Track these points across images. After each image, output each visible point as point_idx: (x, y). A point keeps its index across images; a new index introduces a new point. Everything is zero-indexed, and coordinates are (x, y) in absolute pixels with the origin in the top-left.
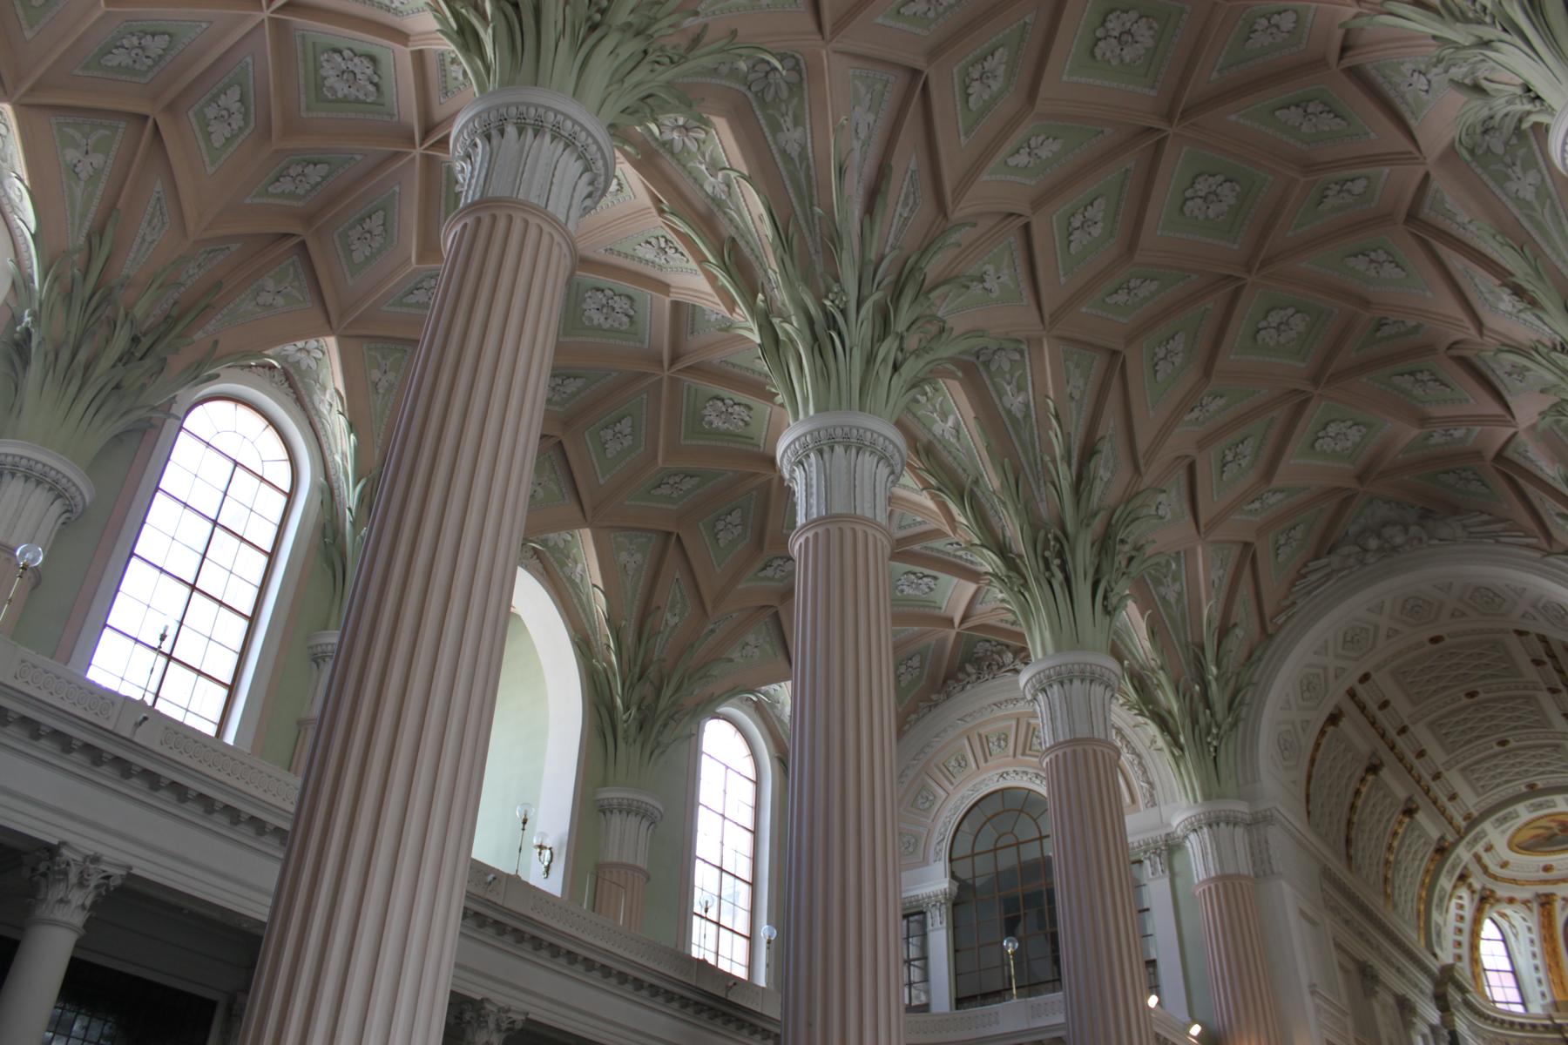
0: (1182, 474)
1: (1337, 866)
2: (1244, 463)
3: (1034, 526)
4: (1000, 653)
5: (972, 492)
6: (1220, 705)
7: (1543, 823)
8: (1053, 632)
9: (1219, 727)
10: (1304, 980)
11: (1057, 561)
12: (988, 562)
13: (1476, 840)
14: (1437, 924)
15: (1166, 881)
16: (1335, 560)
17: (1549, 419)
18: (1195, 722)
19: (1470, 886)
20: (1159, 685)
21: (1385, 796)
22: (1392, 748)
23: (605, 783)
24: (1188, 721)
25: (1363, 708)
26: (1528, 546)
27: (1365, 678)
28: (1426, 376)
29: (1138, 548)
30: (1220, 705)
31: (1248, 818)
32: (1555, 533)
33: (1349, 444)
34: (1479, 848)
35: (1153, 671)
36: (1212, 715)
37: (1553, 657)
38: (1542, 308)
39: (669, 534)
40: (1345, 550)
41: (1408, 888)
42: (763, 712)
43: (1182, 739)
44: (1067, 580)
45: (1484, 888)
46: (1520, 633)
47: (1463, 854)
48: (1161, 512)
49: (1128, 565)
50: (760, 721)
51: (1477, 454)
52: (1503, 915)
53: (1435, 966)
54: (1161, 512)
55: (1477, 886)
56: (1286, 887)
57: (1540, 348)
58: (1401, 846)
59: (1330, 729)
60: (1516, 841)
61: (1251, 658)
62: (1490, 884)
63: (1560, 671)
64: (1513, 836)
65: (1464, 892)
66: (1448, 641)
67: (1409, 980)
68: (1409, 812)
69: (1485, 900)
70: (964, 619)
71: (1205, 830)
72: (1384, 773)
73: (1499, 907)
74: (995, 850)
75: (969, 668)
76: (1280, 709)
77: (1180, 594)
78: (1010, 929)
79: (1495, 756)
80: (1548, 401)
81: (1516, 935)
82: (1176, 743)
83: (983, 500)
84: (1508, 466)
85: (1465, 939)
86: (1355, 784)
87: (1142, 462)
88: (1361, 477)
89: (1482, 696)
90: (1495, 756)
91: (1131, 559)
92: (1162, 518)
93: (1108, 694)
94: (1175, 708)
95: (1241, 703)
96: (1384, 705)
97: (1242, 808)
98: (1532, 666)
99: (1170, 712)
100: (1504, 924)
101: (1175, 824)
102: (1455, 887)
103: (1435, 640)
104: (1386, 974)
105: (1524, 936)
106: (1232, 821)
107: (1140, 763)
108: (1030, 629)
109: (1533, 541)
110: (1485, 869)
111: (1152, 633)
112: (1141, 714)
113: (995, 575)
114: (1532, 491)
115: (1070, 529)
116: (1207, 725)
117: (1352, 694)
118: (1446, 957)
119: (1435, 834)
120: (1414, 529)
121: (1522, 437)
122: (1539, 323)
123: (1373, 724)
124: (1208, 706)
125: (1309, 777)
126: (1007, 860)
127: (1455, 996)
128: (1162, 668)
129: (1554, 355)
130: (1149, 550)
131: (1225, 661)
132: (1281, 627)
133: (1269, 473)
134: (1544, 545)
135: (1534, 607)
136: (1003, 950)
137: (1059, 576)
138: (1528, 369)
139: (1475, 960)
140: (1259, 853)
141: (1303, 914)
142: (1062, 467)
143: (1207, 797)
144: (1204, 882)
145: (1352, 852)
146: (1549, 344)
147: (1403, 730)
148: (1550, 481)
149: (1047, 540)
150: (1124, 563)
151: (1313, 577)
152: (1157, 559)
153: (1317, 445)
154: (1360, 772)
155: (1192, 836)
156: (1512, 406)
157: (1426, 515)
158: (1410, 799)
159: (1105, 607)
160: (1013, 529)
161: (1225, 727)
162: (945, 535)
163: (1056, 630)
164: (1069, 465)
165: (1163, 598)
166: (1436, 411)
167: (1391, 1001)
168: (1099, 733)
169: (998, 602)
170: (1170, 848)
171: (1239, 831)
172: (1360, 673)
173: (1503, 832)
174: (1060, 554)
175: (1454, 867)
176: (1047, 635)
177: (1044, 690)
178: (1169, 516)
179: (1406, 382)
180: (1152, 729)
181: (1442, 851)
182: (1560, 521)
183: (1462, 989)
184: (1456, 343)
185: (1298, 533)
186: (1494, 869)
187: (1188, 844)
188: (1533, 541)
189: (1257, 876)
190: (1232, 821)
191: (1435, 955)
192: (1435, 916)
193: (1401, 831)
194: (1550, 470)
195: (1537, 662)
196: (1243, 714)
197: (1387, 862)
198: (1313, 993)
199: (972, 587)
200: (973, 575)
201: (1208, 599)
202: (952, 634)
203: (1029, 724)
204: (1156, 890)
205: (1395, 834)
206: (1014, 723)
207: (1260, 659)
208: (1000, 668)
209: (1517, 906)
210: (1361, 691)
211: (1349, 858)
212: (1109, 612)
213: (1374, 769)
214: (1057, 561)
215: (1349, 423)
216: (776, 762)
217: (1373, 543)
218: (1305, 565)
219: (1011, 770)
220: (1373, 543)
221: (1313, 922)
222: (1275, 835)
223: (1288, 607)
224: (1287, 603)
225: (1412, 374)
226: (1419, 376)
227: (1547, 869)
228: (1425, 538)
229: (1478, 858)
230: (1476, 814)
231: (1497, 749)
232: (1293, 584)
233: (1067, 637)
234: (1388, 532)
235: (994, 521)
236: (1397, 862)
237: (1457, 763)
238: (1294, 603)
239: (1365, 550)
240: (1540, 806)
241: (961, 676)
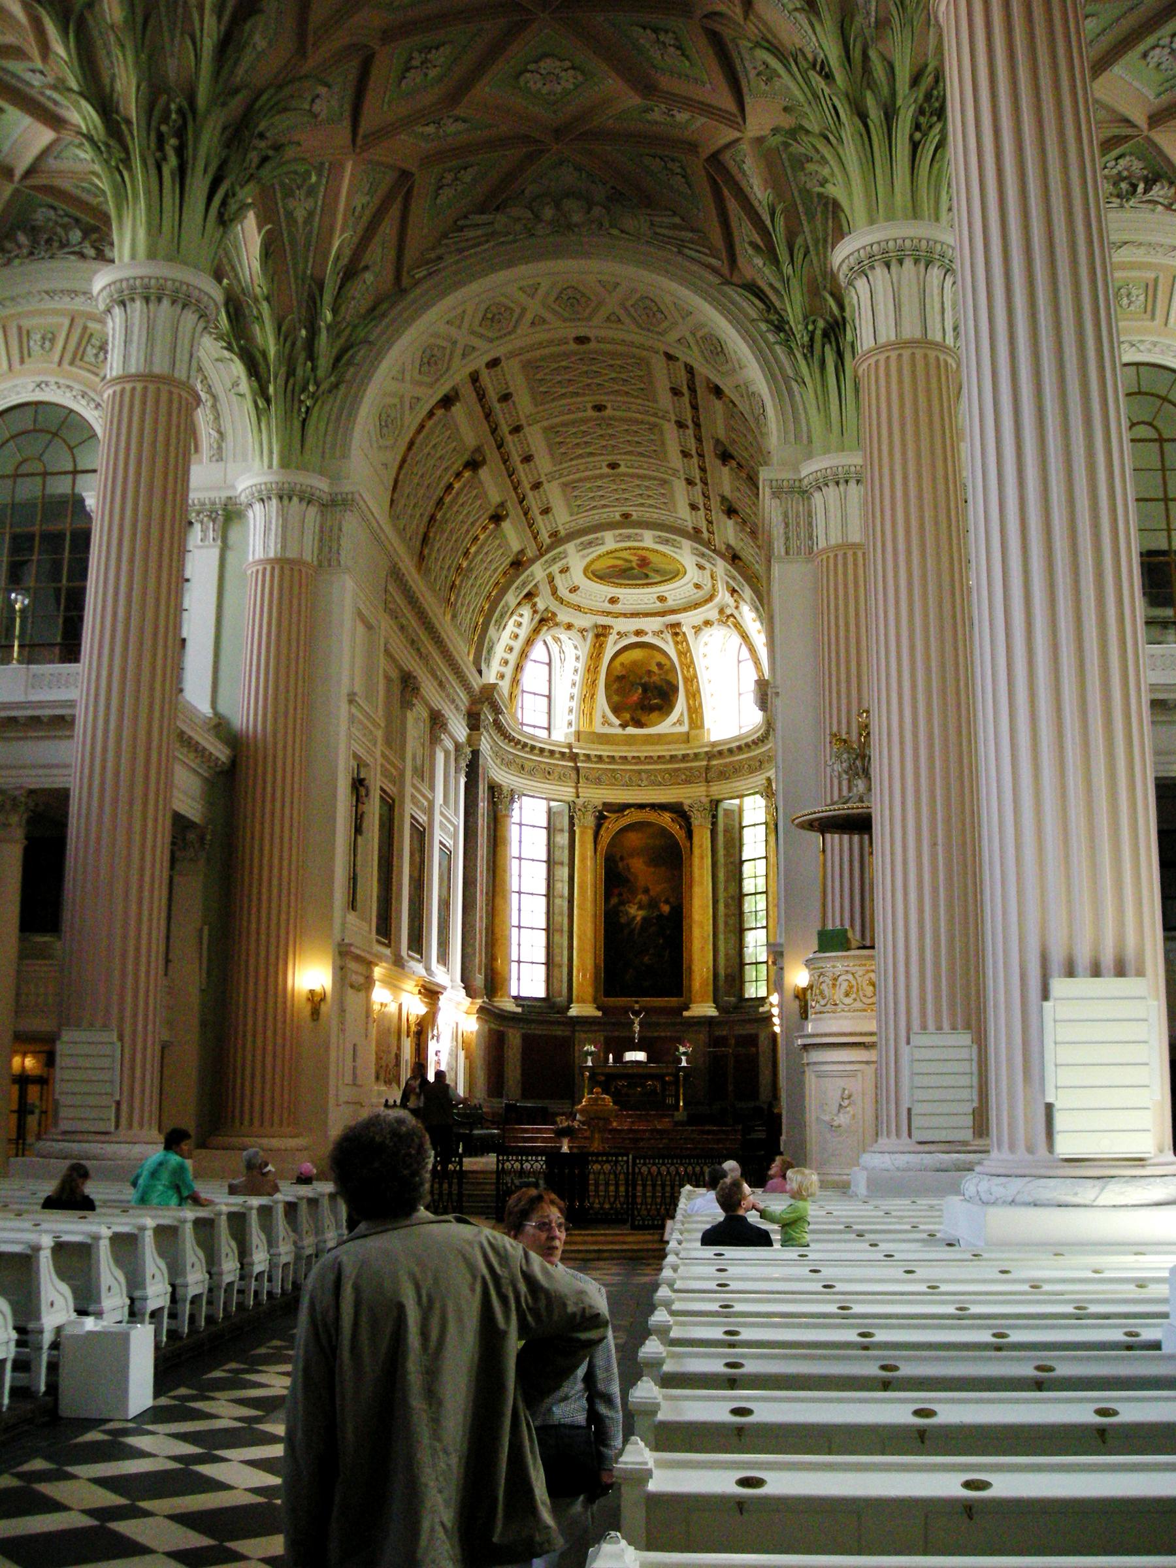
0: (352, 67)
1: (408, 566)
2: (433, 73)
3: (154, 89)
4: (66, 227)
6: (324, 363)
7: (625, 554)
8: (149, 232)
9: (318, 384)
10: (344, 690)
11: (173, 141)
12: (82, 115)
13: (554, 560)
14: (491, 640)
15: (215, 552)
16: (501, 219)
17: (779, 139)
18: (291, 373)
19: (534, 605)
20: (259, 318)
21: (499, 546)
22: (499, 447)
24: (283, 370)
25: (481, 396)
26: (709, 266)
27: (494, 363)
28: (668, 39)
29: (278, 148)
30: (324, 363)
31: (326, 498)
32: (741, 261)
33: (559, 89)
34: (555, 569)
35: (256, 300)
36: (314, 369)
37: (692, 390)
38: (818, 14)
40: (516, 212)
41: (472, 600)
43: (271, 389)
44: (182, 172)
45: (546, 609)
46: (670, 357)
47: (538, 571)
48: (316, 108)
49: (259, 167)
51: (692, 147)
52: (557, 640)
53: (476, 683)
54: (316, 108)
55: (541, 606)
56: (349, 583)
57: (800, 58)
58: (477, 552)
59: (440, 412)
60: (593, 567)
61: (374, 312)
62: (554, 606)
63: (695, 407)
64: (592, 562)
65: (526, 611)
66: (592, 345)
67: (448, 696)
68: (497, 518)
69: (545, 621)
70: (30, 172)
71: (274, 501)
72: (484, 473)
73: (556, 632)
74: (16, 476)
75: (22, 238)
76: (391, 378)
77: (311, 214)
78: (15, 579)
79: (601, 476)
80: (787, 121)
81: (562, 661)
82: (263, 392)
83: (95, 33)
84: (720, 173)
85: (513, 658)
86: (448, 477)
87: (311, 40)
88: (558, 133)
90: (601, 476)
91: (265, 159)
92: (316, 116)
93: (202, 324)
94: (272, 351)
95: (349, 363)
96: (505, 397)
97: (321, 485)
98: (669, 394)
99: (264, 354)
100: (554, 648)
101: (240, 488)
102: (519, 604)
103: (581, 340)
104: (429, 688)
105: (571, 663)
106: (308, 498)
107: (214, 406)
108: (120, 217)
109: (713, 261)
110: (554, 592)
111: (267, 252)
112: (229, 348)
113: (89, 138)
114: (733, 205)
115: (202, 101)
116: (303, 383)
117: (475, 378)
118: (491, 677)
119: (516, 546)
120: (597, 211)
121: (745, 146)
122: (810, 32)
123: (488, 416)
124: (311, 357)
125: (404, 461)
126: (28, 490)
127: (488, 716)
128: (267, 299)
129: (811, 73)
130: (290, 152)
131: (343, 309)
132: (417, 283)
133: (454, 97)
134: (725, 270)
135: (693, 334)
136: (10, 605)
137: (173, 161)
138: (779, 76)
139: (515, 681)
140: (328, 539)
141: (360, 614)
142: (210, 20)
143: (285, 464)
144: (261, 561)
145: (426, 552)
146: (810, 57)
147: (517, 429)
148: (756, 204)
149: (167, 112)
150: (256, 161)
151: (471, 234)
152: (293, 167)
153: (522, 79)
154: (458, 466)
155: (258, 507)
156: (748, 108)
157: (616, 197)
158: (502, 505)
159: (221, 215)
160: (126, 84)
161: (325, 386)
162: (30, 59)
163: (155, 230)
164: (219, 22)
165: (290, 215)
166: (665, 82)
167: (425, 714)
168: (181, 374)
169: (83, 164)
170: (229, 515)
171: (312, 511)
172: (487, 358)
173: (584, 557)
174: (180, 133)
175: (524, 584)
176: (142, 233)
177: (123, 303)
178: (323, 116)
179: (645, 38)
180: (238, 368)
181: (518, 564)
182: (750, 251)
183: (496, 710)
184: (716, 14)
185: (467, 177)
186: (563, 591)
187: (250, 514)
188: (713, 261)
189: (320, 561)
190: (308, 498)
191: (480, 672)
192: (492, 631)
193: (482, 537)
194: (760, 192)
195: (676, 392)
196: (348, 377)
197: (459, 567)
198: (351, 702)
199: (46, 136)
200: (55, 121)
201: (343, 231)
202: (8, 190)
203: (85, 328)
204: (201, 562)
205: (476, 538)
206: (67, 322)
207: (383, 315)
208: (62, 246)
209: (573, 633)
210: (486, 378)
211: (422, 557)
212: (225, 221)
213: (473, 465)
214: (173, 141)
215: (568, 64)
217: (548, 213)
218: (466, 217)
219: (52, 380)
220: (548, 213)
221: (369, 627)
222: (350, 524)
223: (432, 261)
224: (433, 256)
225: (655, 30)
226: (662, 37)
227: (613, 601)
228: (607, 224)
229: (551, 579)
230: (563, 533)
231: (606, 470)
232: (445, 235)
233: (165, 244)
234: (570, 204)
235: (104, 63)
236: (470, 569)
237: (561, 476)
238: (440, 258)
239: (538, 218)
240: (629, 537)
241: (9, 245)
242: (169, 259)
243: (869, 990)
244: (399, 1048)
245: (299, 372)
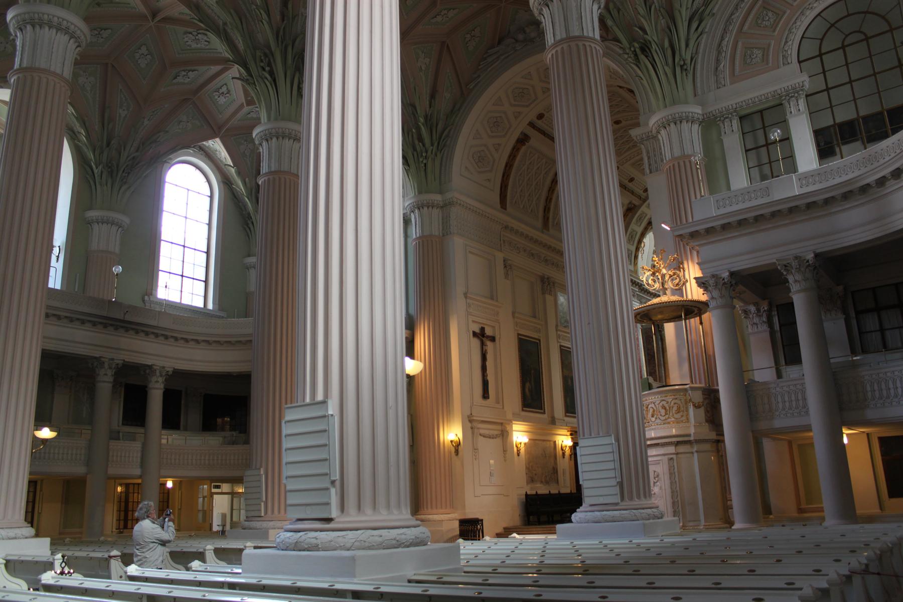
5: (224, 29)
18: (415, 149)
23: (91, 208)
30: (427, 141)
31: (441, 204)
39: (107, 64)
42: (210, 157)
50: (210, 163)
71: (416, 211)
89: (624, 123)
106: (430, 205)
143: (420, 192)
171: (436, 211)
174: (269, 65)
207: (459, 110)
216: (222, 185)
217: (521, 37)
220: (521, 37)
238: (479, 76)
239: (517, 41)
242: (276, 119)
243: (663, 411)
244: (556, 463)
245: (418, 148)
